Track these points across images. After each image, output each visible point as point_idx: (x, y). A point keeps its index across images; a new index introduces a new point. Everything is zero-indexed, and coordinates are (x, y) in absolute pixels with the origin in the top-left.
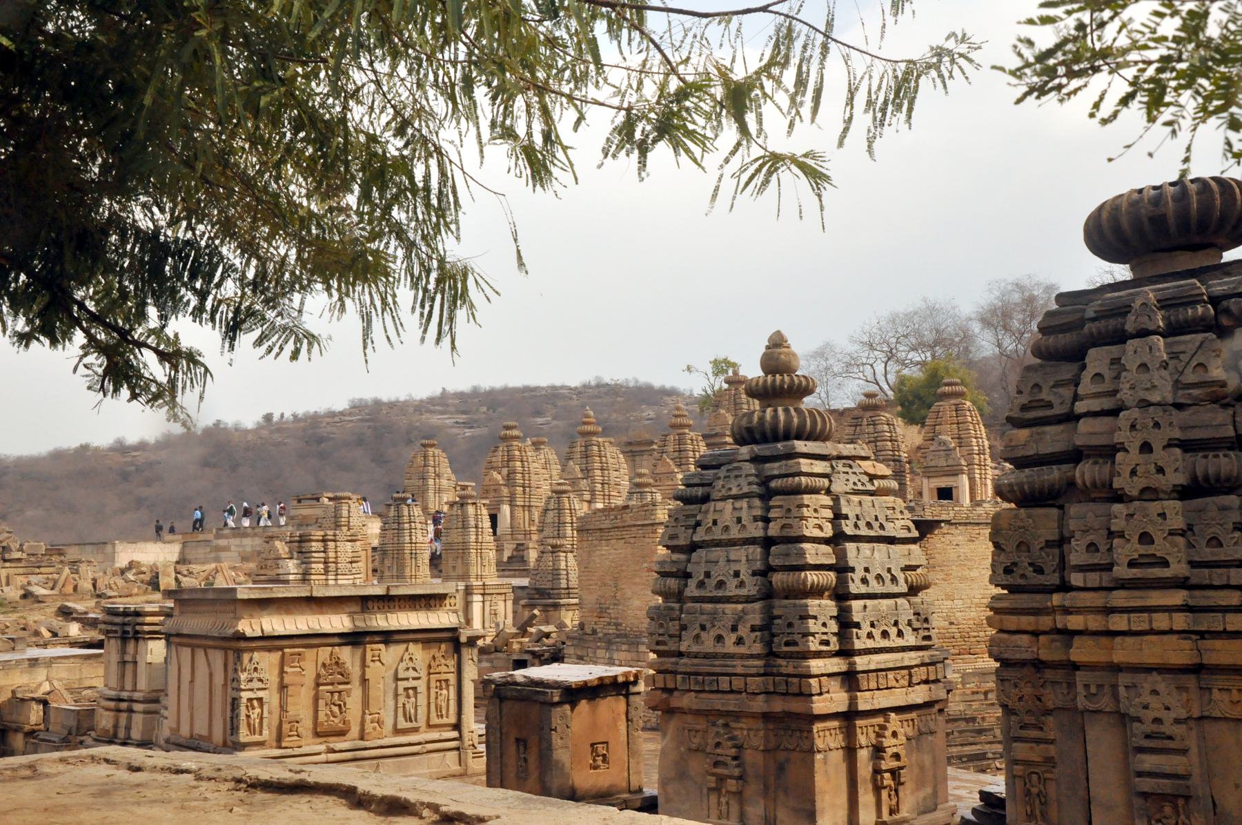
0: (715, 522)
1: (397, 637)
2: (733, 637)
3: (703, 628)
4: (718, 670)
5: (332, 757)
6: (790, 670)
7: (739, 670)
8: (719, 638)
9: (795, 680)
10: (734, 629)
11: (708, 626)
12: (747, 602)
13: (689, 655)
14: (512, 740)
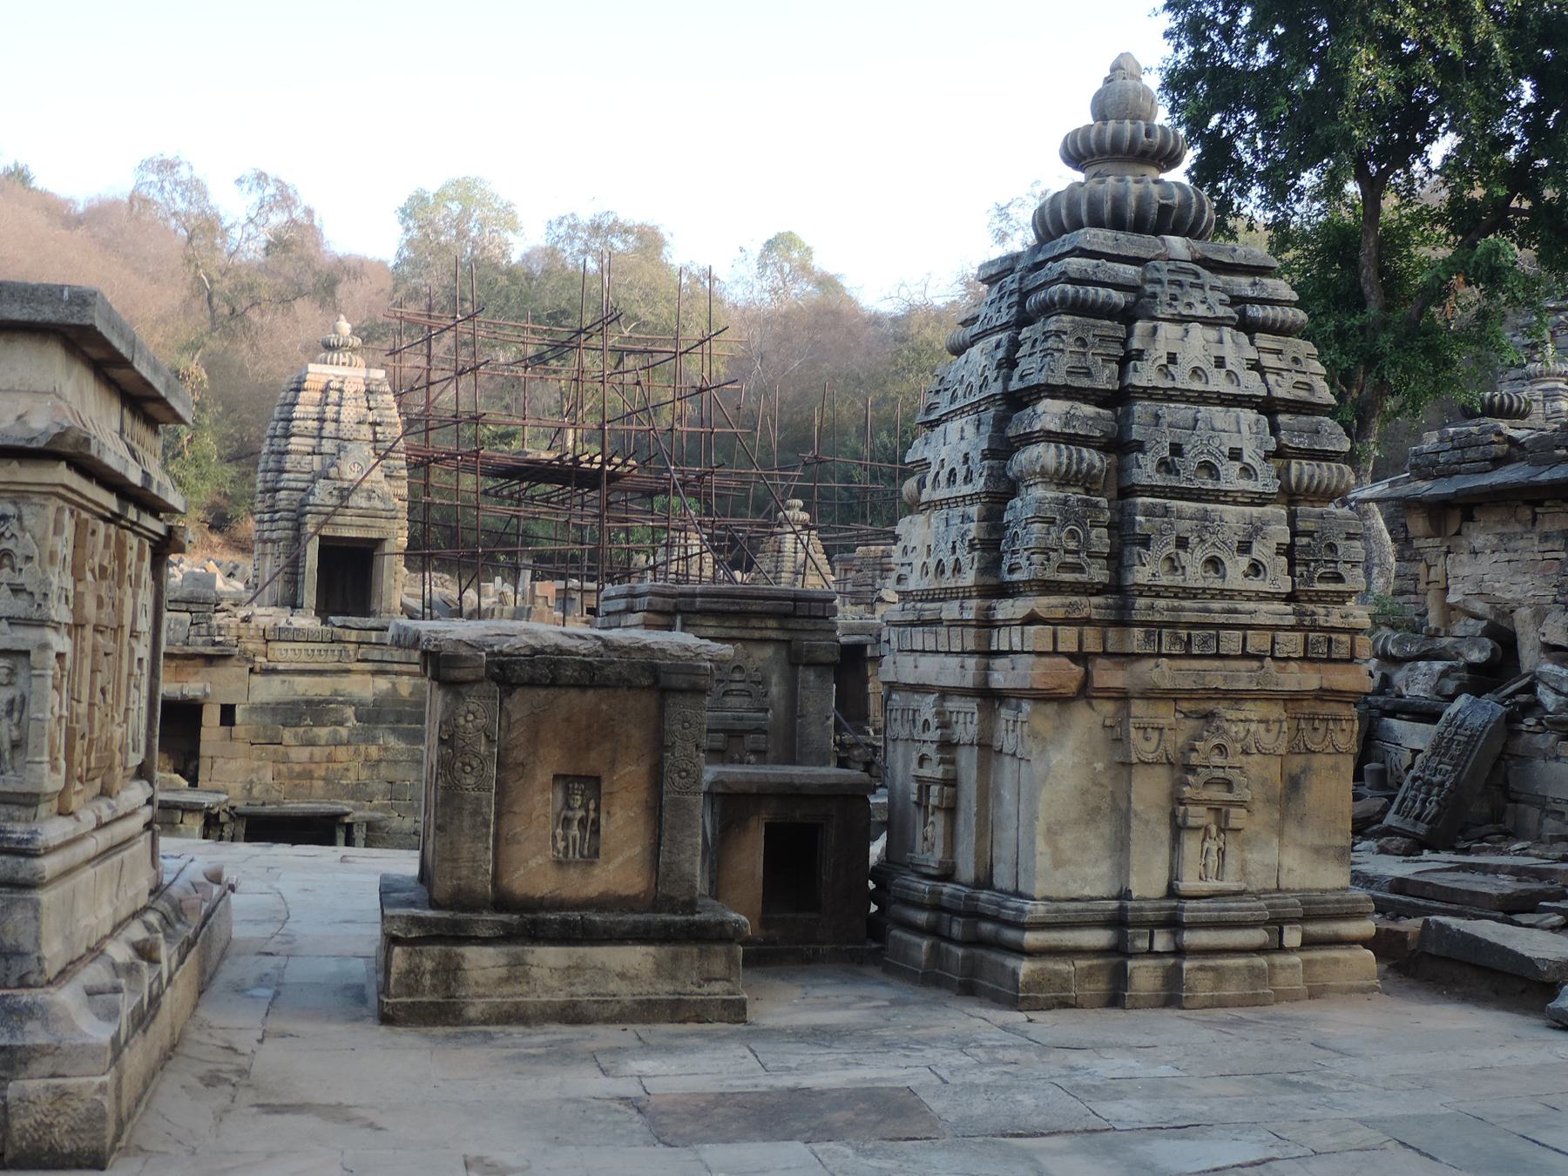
0: (1172, 358)
2: (1244, 562)
3: (1182, 543)
4: (1221, 619)
6: (1335, 621)
7: (1261, 619)
8: (1214, 563)
9: (1345, 638)
10: (1244, 548)
11: (1193, 540)
12: (1252, 504)
13: (1155, 592)
14: (544, 775)
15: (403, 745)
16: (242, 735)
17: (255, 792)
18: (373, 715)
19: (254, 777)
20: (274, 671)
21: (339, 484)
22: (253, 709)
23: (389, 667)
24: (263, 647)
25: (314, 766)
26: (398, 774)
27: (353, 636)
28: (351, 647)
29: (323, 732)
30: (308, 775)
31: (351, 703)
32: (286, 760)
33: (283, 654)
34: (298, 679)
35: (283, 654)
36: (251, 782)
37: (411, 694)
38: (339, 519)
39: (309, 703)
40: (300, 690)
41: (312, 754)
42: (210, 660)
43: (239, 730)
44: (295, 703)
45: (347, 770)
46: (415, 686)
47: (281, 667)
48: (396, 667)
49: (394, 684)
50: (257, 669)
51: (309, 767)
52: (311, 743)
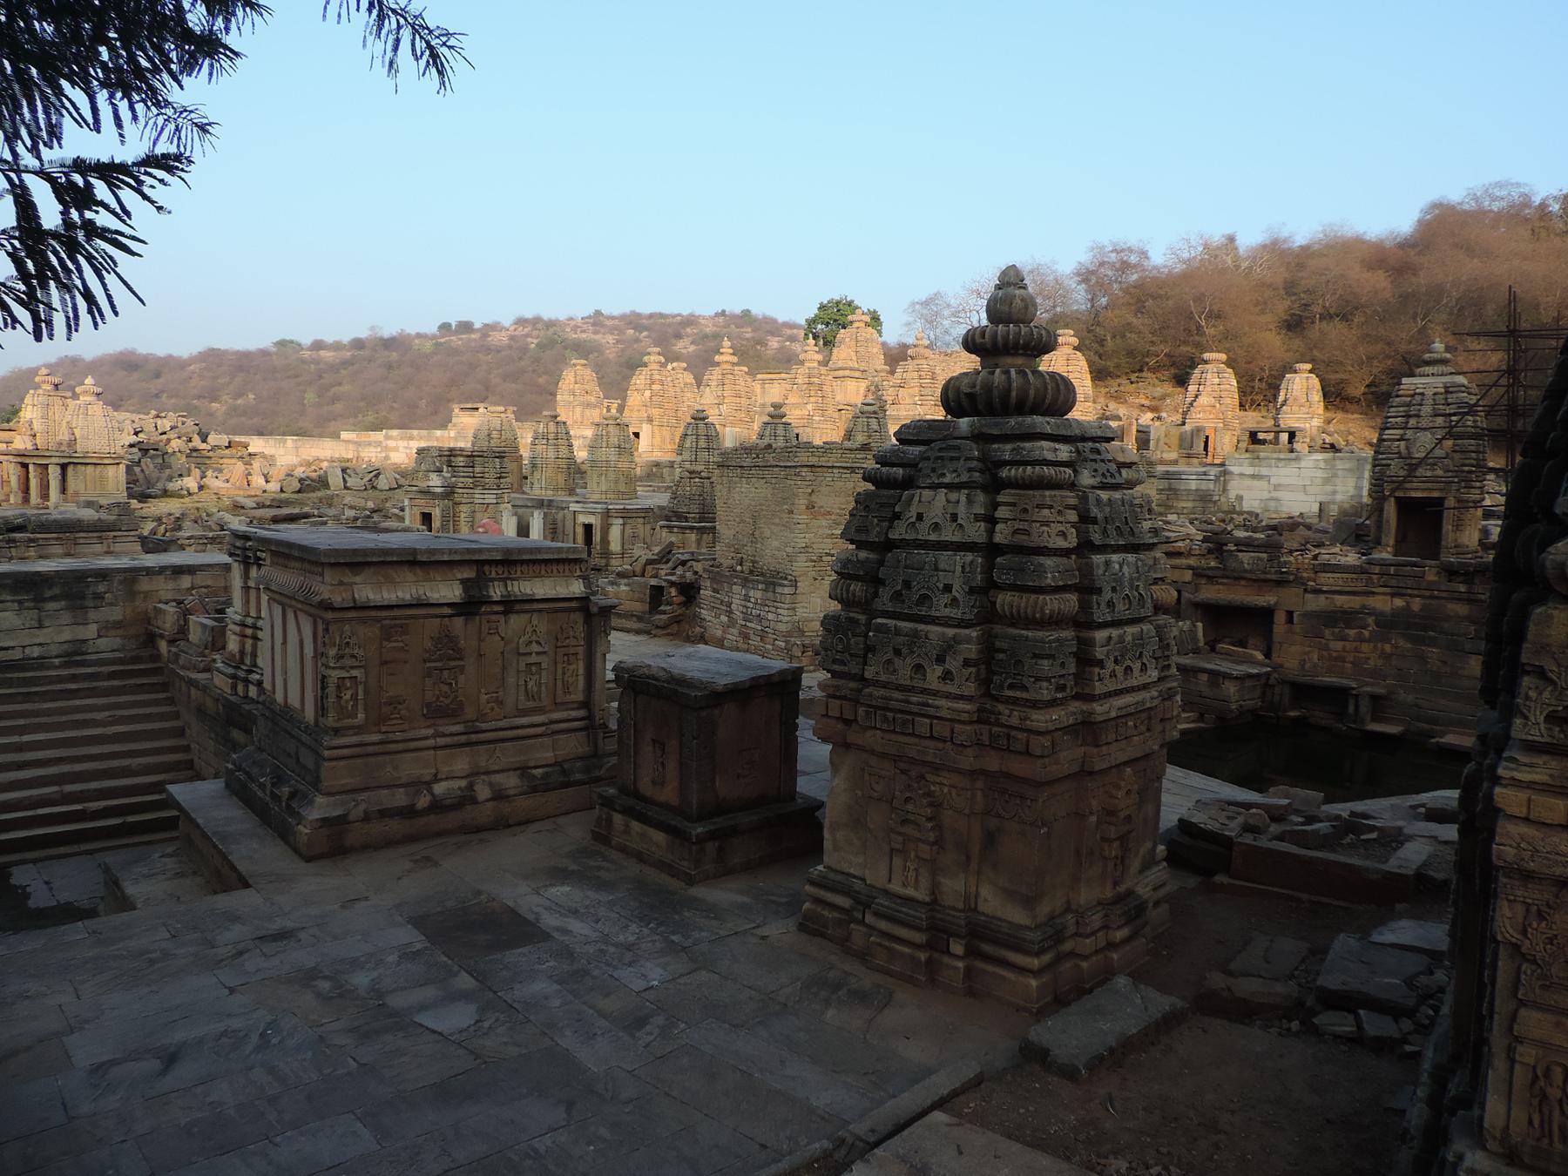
0: (920, 517)
1: (517, 607)
2: (939, 670)
3: (898, 652)
4: (915, 709)
5: (441, 741)
6: (1015, 721)
7: (944, 714)
8: (919, 668)
9: (1021, 736)
10: (940, 660)
11: (905, 651)
12: (958, 626)
13: (876, 683)
17: (1307, 666)
18: (1388, 623)
20: (1317, 591)
29: (1352, 632)
30: (1343, 660)
32: (1327, 648)
33: (1327, 580)
34: (1337, 597)
35: (1327, 580)
38: (1408, 485)
39: (1344, 612)
42: (1280, 583)
43: (1297, 628)
52: (1344, 639)
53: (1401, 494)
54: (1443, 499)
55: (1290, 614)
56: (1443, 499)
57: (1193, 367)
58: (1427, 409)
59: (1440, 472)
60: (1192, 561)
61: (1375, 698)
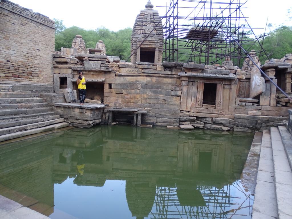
15: (153, 94)
16: (113, 91)
17: (117, 105)
18: (145, 87)
19: (117, 101)
21: (145, 35)
22: (116, 85)
23: (150, 75)
24: (118, 69)
25: (131, 99)
26: (152, 101)
27: (141, 66)
28: (140, 69)
30: (130, 102)
31: (140, 83)
34: (127, 77)
35: (123, 71)
36: (116, 103)
37: (156, 81)
38: (145, 43)
39: (129, 83)
40: (128, 80)
41: (130, 96)
42: (106, 72)
43: (113, 90)
44: (126, 83)
45: (139, 100)
46: (157, 79)
47: (123, 74)
48: (152, 75)
49: (151, 79)
50: (117, 75)
51: (130, 99)
53: (142, 46)
54: (155, 48)
55: (110, 85)
56: (155, 48)
57: (74, 38)
58: (148, 20)
59: (154, 39)
60: (71, 66)
61: (143, 115)
